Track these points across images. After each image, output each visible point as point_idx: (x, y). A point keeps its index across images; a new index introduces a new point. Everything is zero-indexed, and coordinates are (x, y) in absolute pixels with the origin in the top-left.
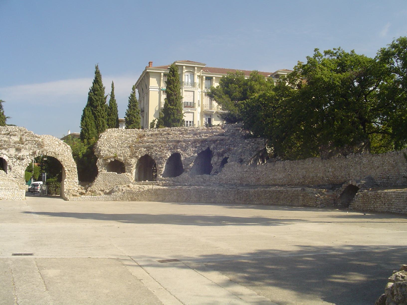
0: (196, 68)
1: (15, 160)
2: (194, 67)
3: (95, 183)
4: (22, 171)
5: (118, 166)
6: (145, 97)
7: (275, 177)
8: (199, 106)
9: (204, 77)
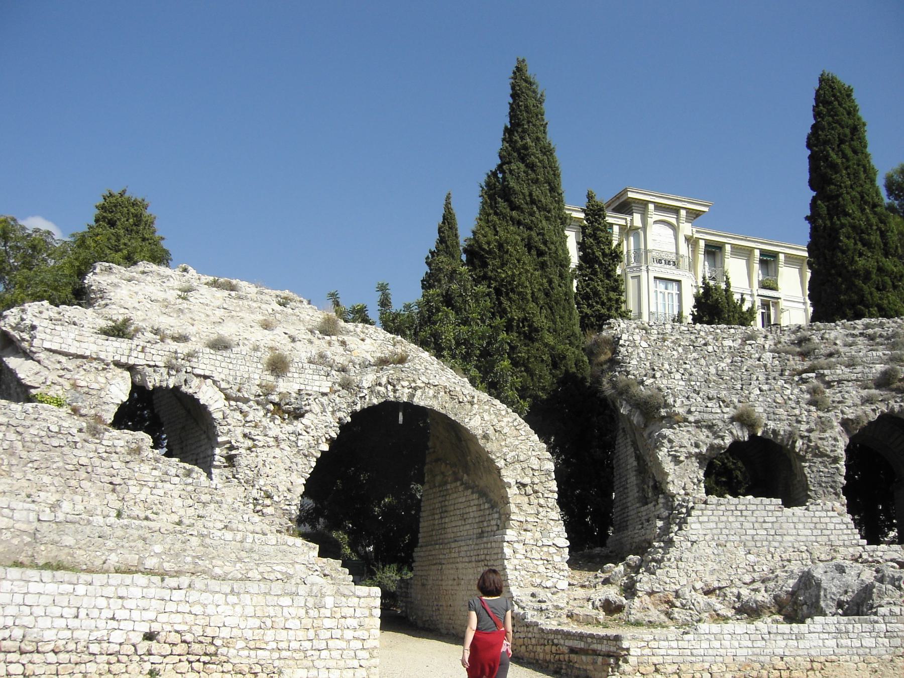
0: (683, 213)
1: (257, 414)
2: (676, 210)
3: (673, 553)
9: (702, 244)
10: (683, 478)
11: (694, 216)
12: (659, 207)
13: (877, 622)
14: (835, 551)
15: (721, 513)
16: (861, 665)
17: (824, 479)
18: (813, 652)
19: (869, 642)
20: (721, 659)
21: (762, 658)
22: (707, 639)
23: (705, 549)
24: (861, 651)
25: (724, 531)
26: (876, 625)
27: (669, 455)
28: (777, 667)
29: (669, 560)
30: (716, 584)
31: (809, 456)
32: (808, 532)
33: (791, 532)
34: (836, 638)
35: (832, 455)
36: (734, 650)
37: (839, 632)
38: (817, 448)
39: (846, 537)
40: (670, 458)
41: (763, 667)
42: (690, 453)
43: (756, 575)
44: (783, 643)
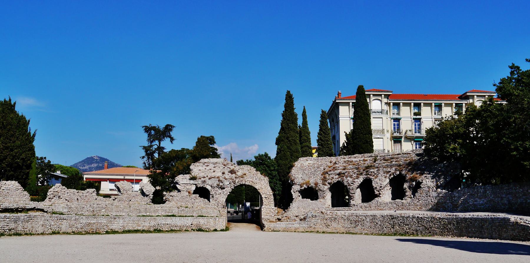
0: (383, 96)
2: (381, 95)
3: (290, 210)
4: (223, 199)
5: (310, 193)
6: (336, 127)
7: (475, 203)
8: (388, 131)
9: (392, 104)
10: (296, 195)
11: (387, 96)
23: (296, 209)
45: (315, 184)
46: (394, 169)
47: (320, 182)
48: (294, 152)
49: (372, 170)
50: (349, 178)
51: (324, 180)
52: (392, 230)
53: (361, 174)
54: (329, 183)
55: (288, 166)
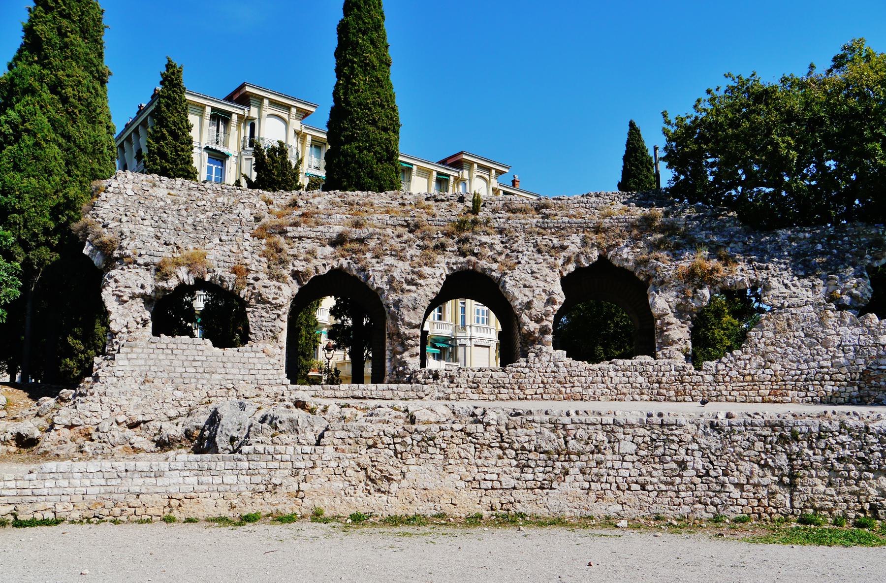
3: (98, 388)
12: (272, 103)
13: (240, 460)
14: (260, 389)
15: (151, 351)
16: (221, 502)
17: (264, 324)
18: (172, 490)
19: (230, 479)
20: (68, 498)
21: (115, 496)
22: (53, 478)
23: (131, 384)
24: (221, 488)
25: (153, 368)
26: (239, 463)
27: (114, 295)
28: (131, 505)
29: (92, 394)
30: (140, 418)
31: (253, 302)
32: (236, 371)
33: (219, 370)
34: (198, 475)
35: (273, 302)
36: (84, 489)
37: (201, 469)
38: (260, 295)
39: (271, 377)
40: (115, 297)
41: (116, 505)
42: (134, 294)
43: (181, 410)
44: (141, 481)
45: (234, 271)
46: (576, 239)
47: (258, 265)
48: (83, 151)
49: (485, 239)
50: (389, 260)
51: (276, 257)
52: (783, 497)
53: (442, 247)
54: (296, 275)
55: (50, 203)
